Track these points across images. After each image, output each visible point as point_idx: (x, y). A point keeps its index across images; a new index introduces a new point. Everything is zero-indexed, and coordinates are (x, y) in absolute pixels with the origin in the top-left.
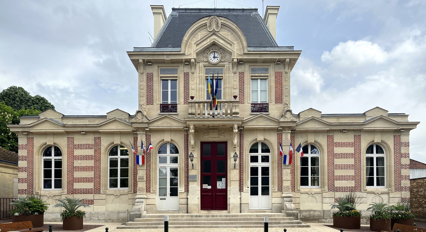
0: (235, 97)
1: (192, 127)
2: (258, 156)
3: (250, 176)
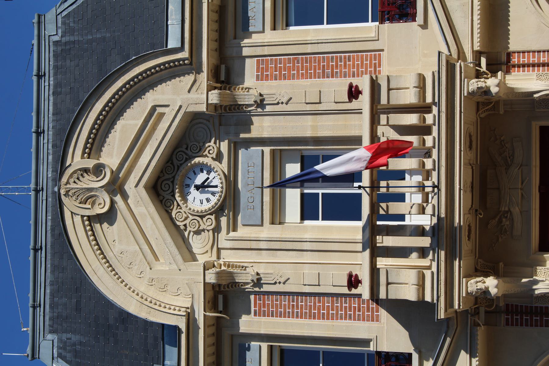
1: (475, 285)
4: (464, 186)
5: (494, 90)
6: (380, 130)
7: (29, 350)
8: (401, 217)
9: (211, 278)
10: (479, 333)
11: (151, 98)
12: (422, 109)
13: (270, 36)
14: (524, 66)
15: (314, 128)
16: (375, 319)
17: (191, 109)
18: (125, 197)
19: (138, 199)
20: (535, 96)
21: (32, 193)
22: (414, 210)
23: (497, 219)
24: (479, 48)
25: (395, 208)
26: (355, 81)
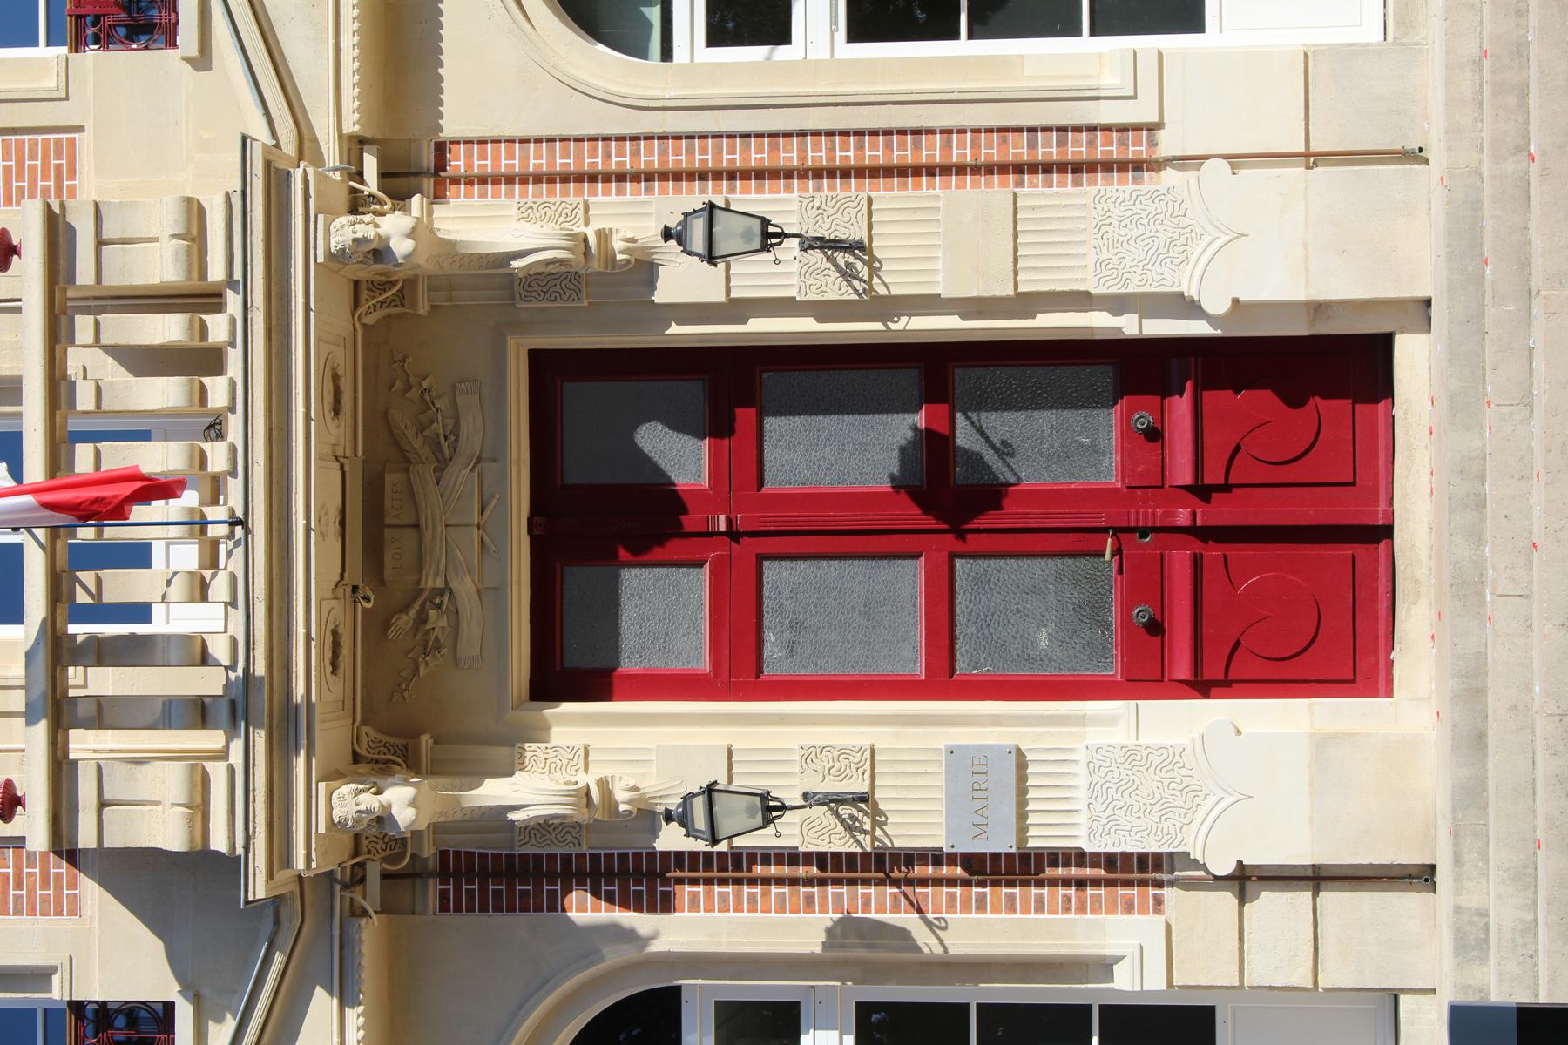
1: (350, 801)
3: (963, 47)
4: (319, 520)
5: (401, 247)
6: (75, 361)
8: (141, 612)
10: (365, 936)
14: (483, 180)
16: (64, 906)
20: (516, 264)
22: (177, 590)
23: (413, 613)
24: (357, 128)
25: (121, 585)
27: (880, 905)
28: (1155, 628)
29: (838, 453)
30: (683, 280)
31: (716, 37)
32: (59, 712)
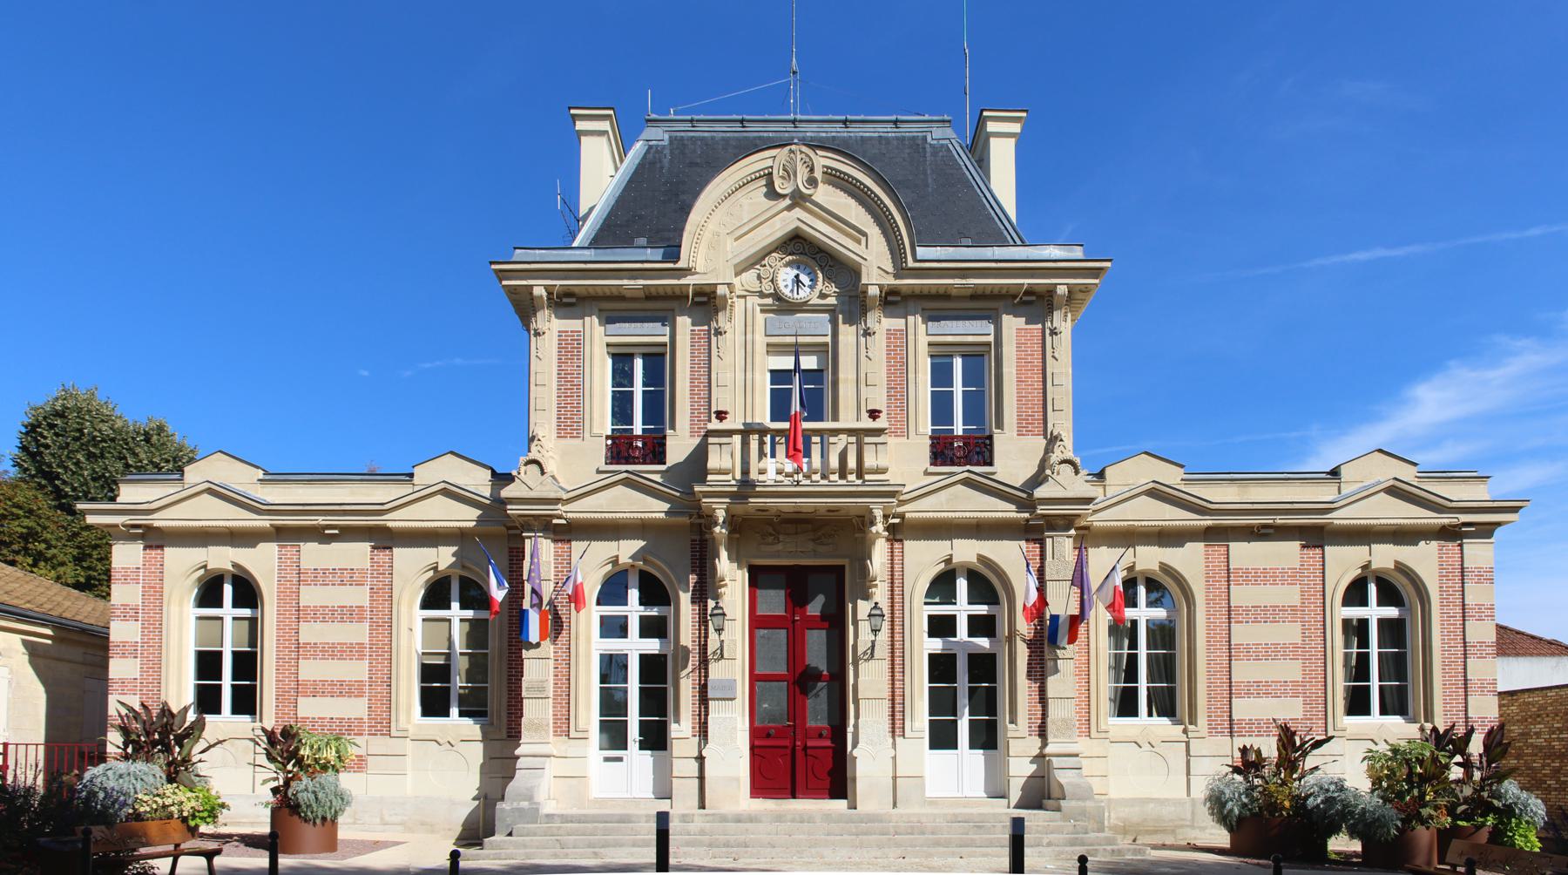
0: (874, 414)
1: (721, 515)
2: (954, 617)
3: (926, 685)
5: (874, 529)
6: (843, 437)
7: (654, 116)
8: (773, 455)
9: (721, 290)
11: (874, 232)
12: (860, 472)
13: (923, 341)
15: (846, 380)
17: (864, 270)
18: (789, 208)
19: (787, 221)
21: (792, 117)
25: (781, 450)
26: (883, 416)
27: (693, 660)
28: (768, 736)
29: (816, 646)
30: (864, 607)
31: (930, 617)
32: (746, 432)
